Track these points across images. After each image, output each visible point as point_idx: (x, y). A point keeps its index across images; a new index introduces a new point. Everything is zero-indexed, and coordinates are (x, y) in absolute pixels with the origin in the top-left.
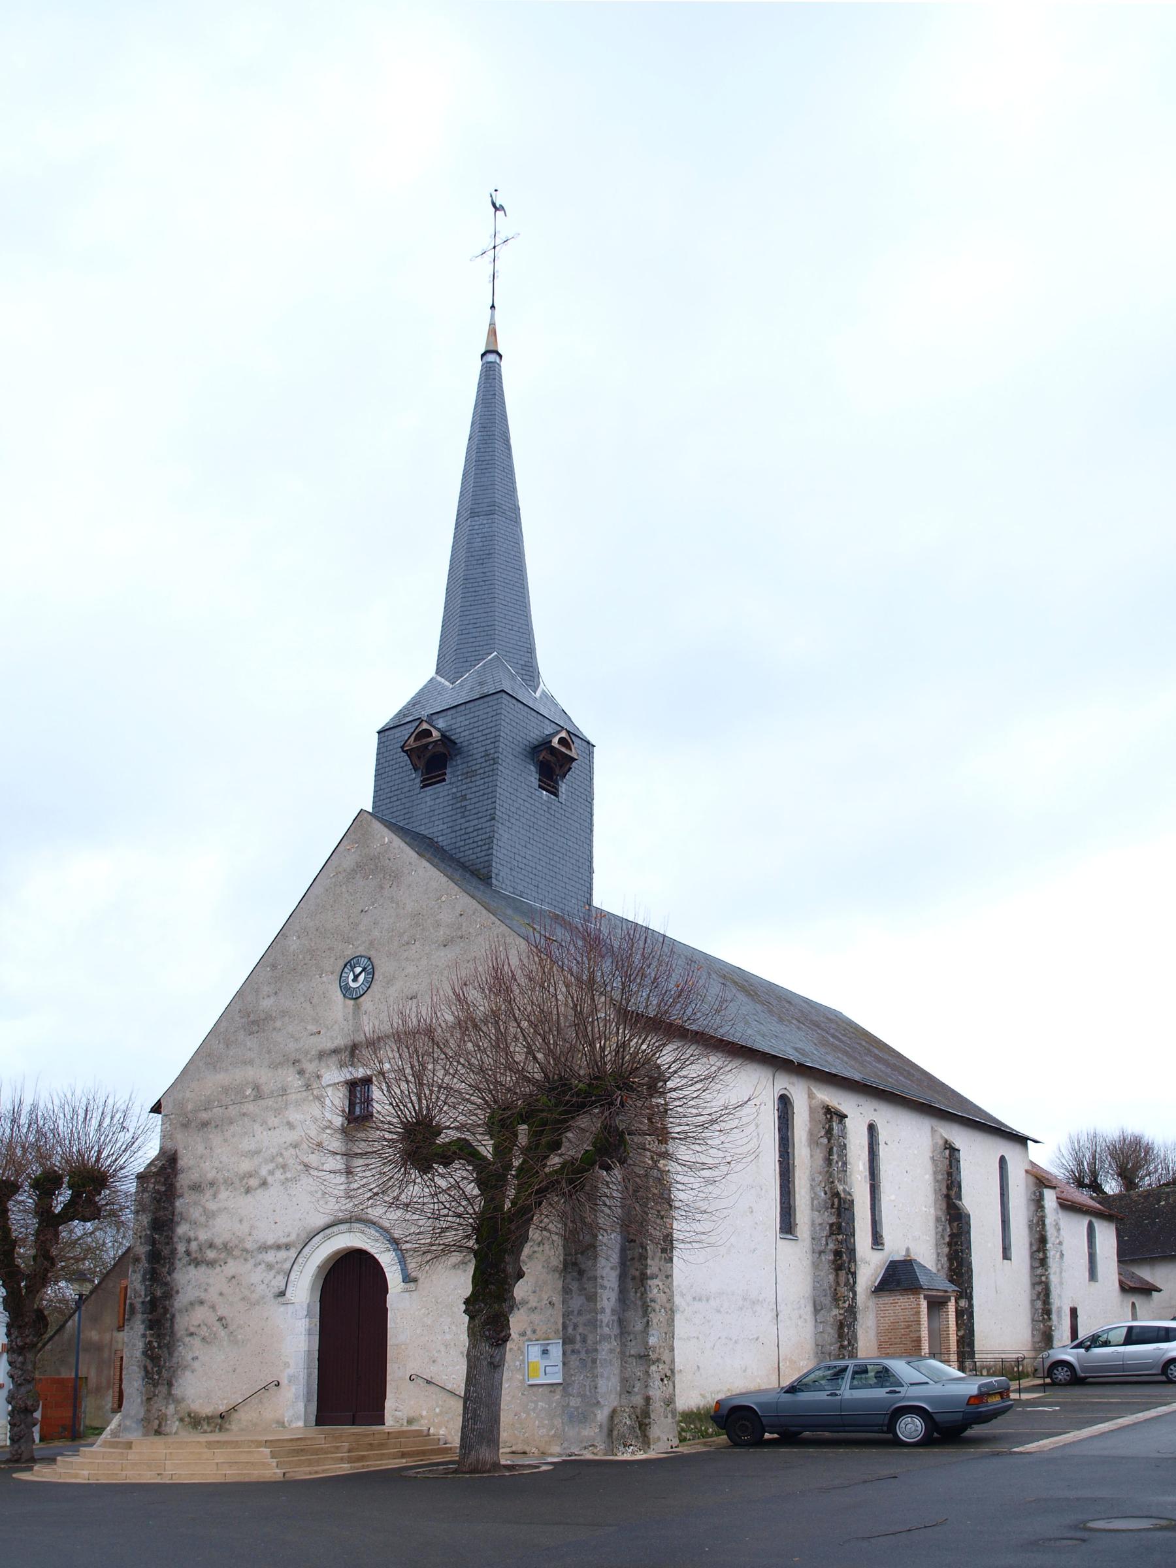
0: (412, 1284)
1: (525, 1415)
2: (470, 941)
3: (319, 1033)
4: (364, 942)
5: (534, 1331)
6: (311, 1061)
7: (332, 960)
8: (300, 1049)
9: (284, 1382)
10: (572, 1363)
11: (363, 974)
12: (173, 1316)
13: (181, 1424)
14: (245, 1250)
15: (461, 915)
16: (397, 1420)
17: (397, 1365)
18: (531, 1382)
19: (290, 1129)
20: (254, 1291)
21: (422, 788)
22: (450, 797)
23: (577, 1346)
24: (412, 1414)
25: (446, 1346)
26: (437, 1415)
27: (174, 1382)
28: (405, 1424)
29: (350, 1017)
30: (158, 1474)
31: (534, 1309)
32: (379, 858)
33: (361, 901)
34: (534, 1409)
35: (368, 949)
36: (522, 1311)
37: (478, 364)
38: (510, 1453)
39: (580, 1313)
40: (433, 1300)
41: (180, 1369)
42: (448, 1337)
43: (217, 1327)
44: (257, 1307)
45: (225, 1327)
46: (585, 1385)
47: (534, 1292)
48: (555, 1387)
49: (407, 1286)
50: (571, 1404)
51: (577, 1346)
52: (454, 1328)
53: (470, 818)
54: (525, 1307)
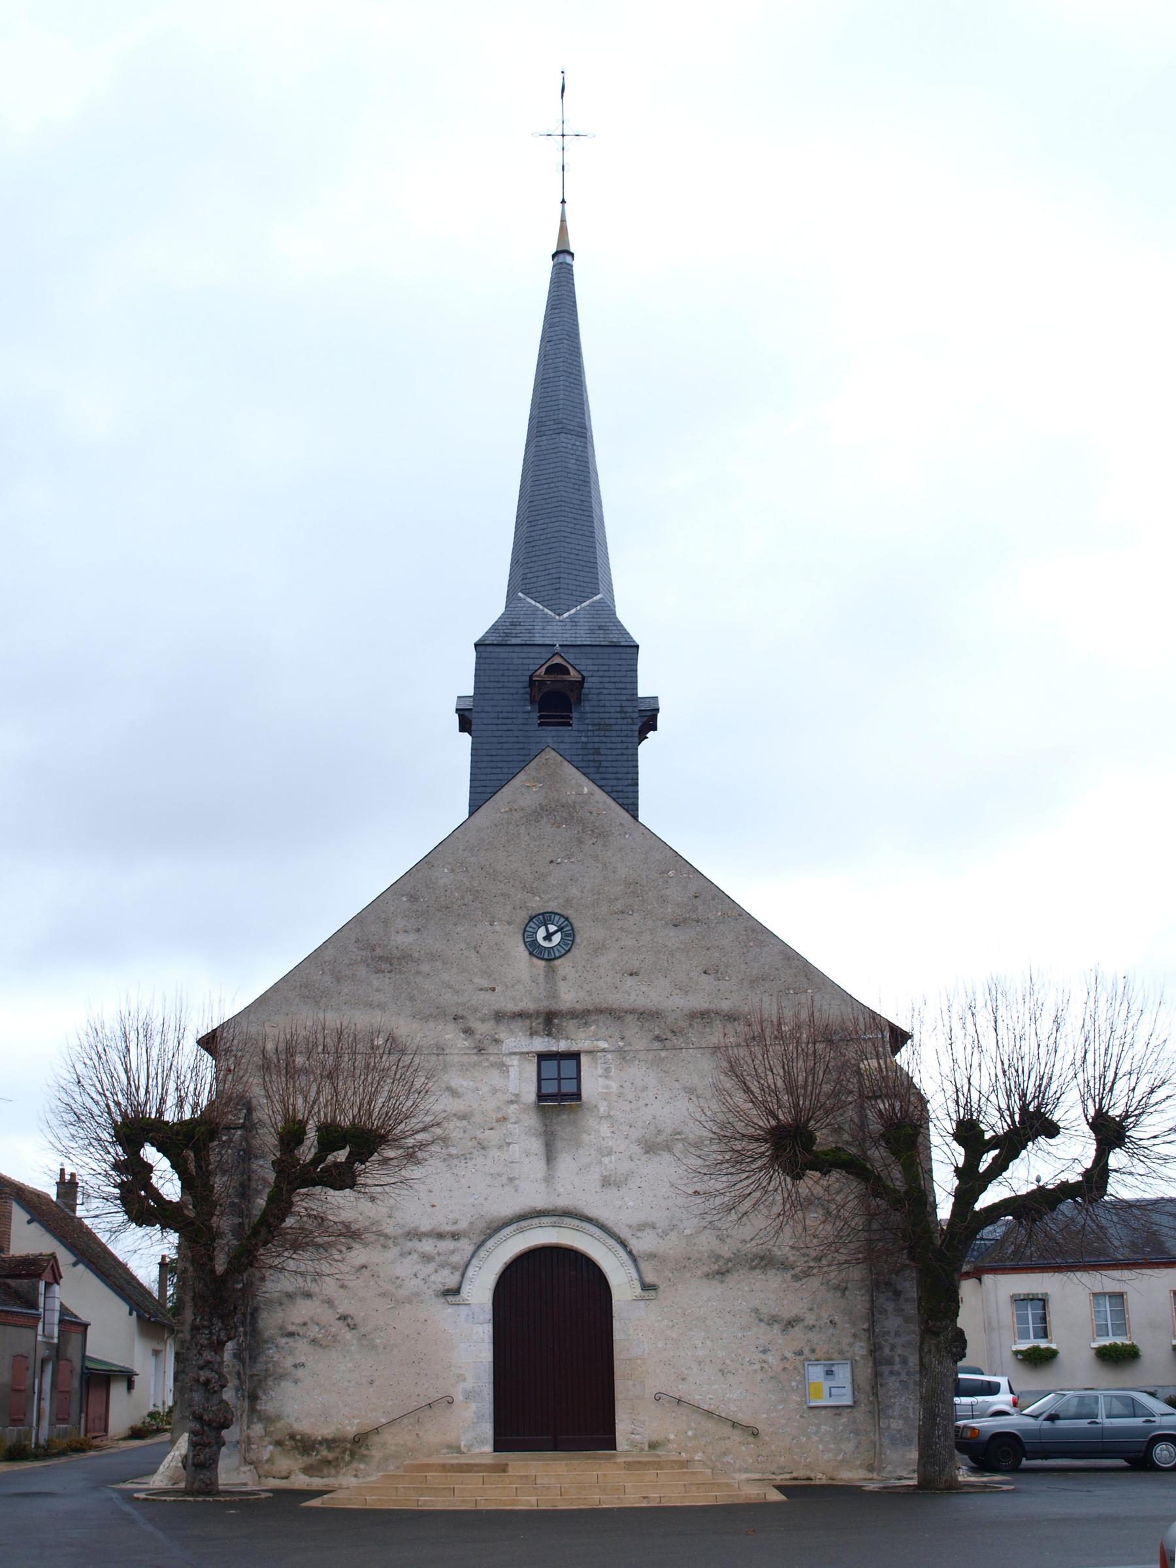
0: (652, 1293)
1: (805, 1439)
2: (708, 927)
3: (493, 990)
4: (557, 898)
5: (813, 1351)
6: (483, 1021)
7: (509, 908)
8: (465, 1004)
9: (459, 1398)
10: (891, 1384)
11: (559, 934)
12: (256, 1310)
13: (279, 1448)
14: (380, 1234)
15: (696, 897)
16: (634, 1444)
17: (631, 1383)
18: (812, 1404)
19: (453, 1096)
20: (400, 1286)
21: (540, 725)
22: (579, 746)
23: (897, 1367)
24: (655, 1438)
25: (700, 1363)
26: (690, 1439)
27: (260, 1393)
28: (646, 1448)
29: (541, 979)
30: (644, 1498)
31: (811, 1328)
32: (574, 808)
33: (550, 850)
34: (816, 1433)
35: (563, 906)
36: (796, 1328)
37: (549, 264)
38: (791, 1479)
39: (897, 1334)
40: (679, 1311)
41: (272, 1378)
42: (701, 1353)
43: (338, 1327)
44: (408, 1306)
45: (353, 1327)
46: (907, 1408)
47: (811, 1310)
48: (840, 1409)
49: (645, 1294)
50: (892, 1426)
51: (897, 1367)
52: (709, 1343)
53: (607, 776)
54: (801, 1325)
